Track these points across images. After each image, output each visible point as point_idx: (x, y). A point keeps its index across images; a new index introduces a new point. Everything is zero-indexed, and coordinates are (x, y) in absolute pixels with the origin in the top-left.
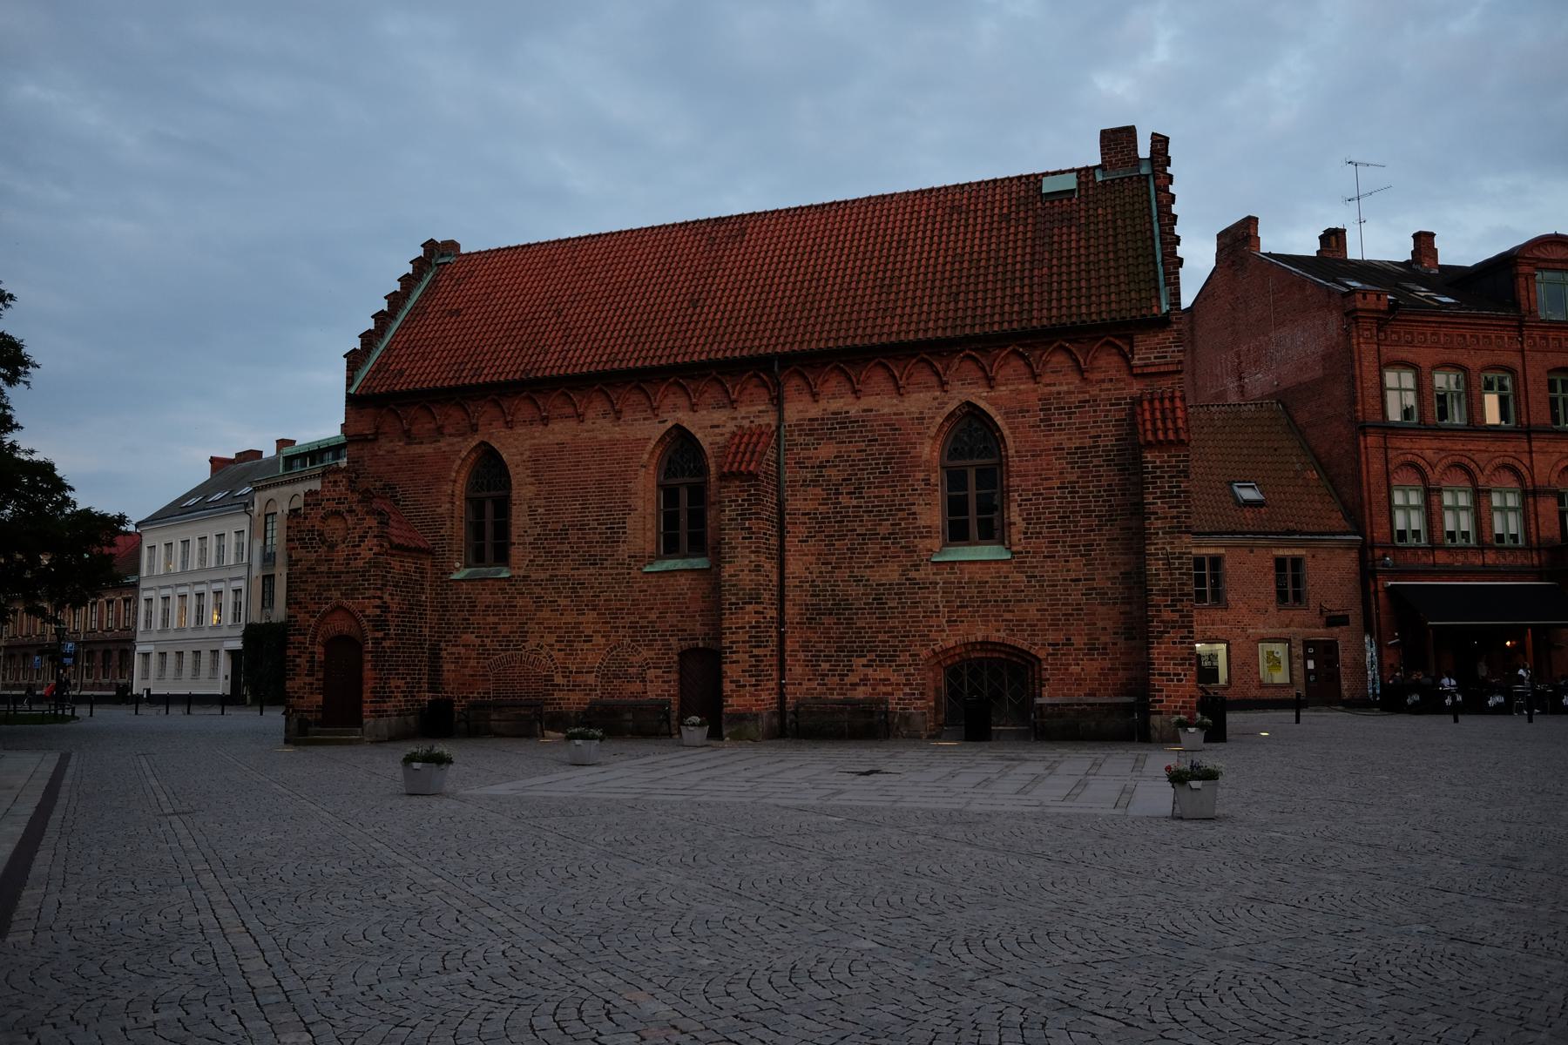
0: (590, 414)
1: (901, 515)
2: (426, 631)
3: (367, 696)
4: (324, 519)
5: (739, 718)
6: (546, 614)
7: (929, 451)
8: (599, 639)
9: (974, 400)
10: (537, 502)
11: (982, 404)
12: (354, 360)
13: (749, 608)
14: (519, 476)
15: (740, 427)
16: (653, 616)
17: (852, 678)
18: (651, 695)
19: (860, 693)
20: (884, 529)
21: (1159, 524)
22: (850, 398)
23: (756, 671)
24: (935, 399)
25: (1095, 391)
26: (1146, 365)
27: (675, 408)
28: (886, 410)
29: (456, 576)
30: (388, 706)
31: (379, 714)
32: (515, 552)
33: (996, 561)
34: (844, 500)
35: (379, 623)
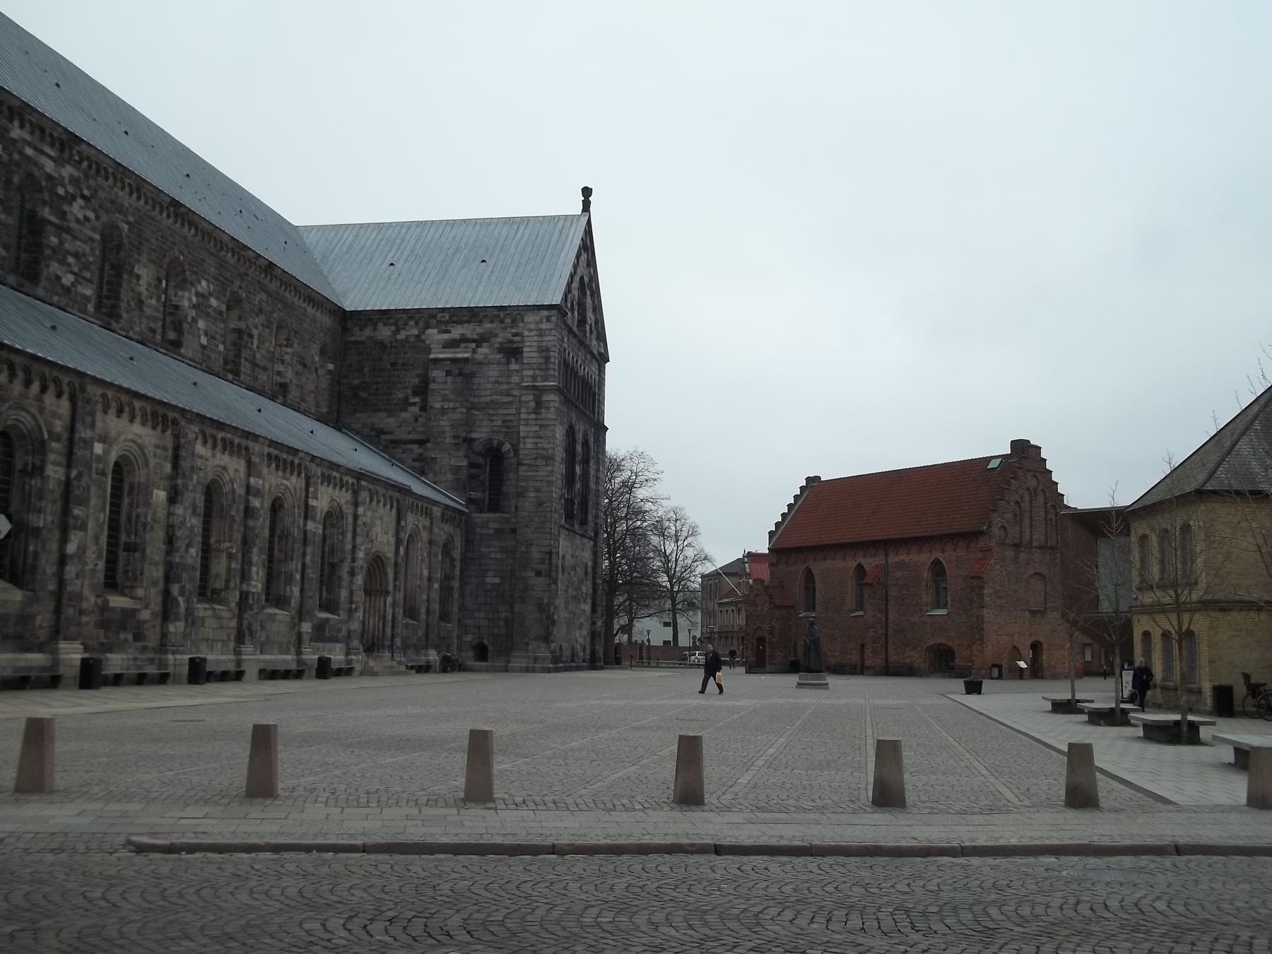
5: (868, 668)
7: (926, 575)
12: (771, 534)
14: (817, 579)
19: (908, 660)
35: (771, 633)
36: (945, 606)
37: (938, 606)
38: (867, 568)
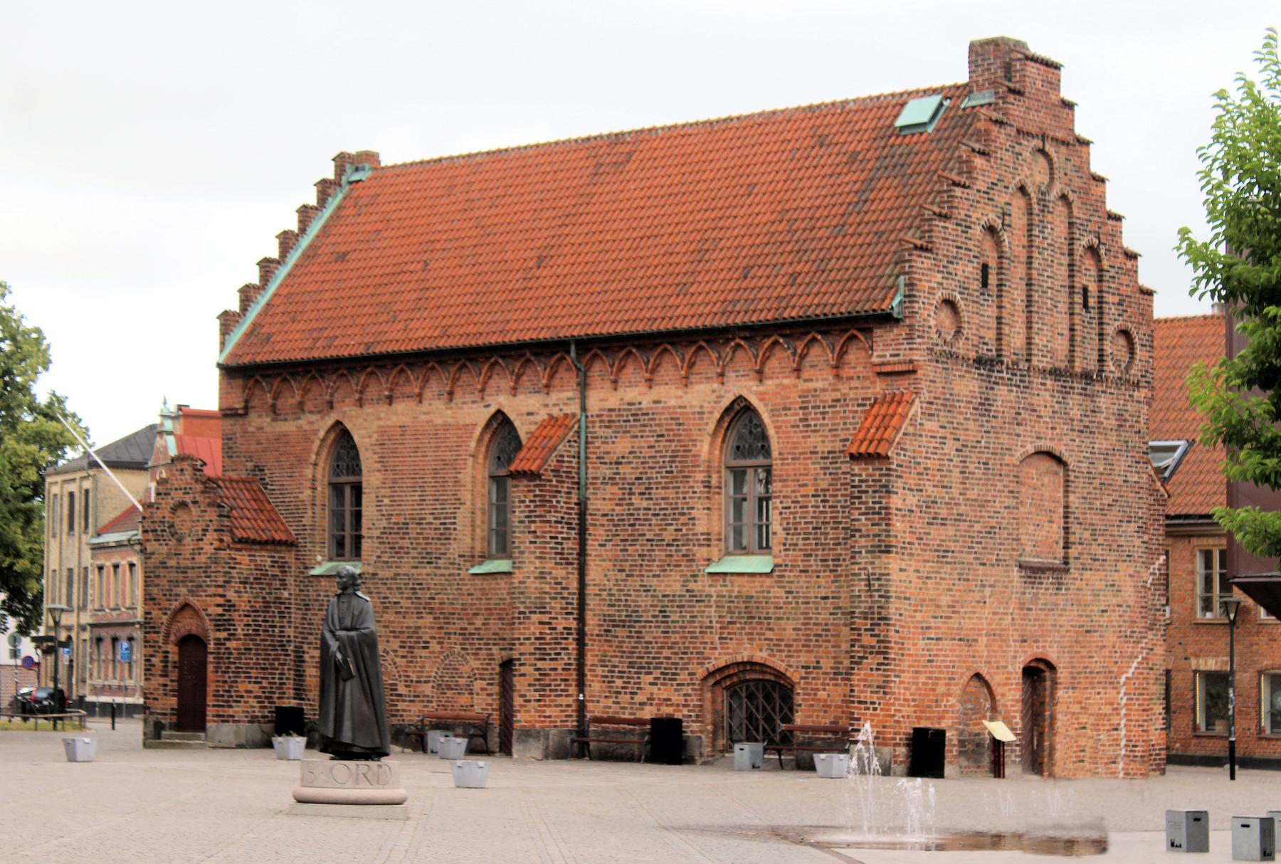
0: (428, 393)
1: (683, 519)
2: (290, 632)
3: (210, 700)
4: (174, 509)
5: (527, 734)
6: (389, 616)
7: (706, 448)
8: (434, 646)
9: (745, 394)
10: (383, 492)
11: (755, 401)
12: (228, 321)
13: (534, 618)
14: (368, 460)
15: (551, 417)
16: (479, 623)
17: (640, 698)
18: (477, 709)
20: (668, 535)
21: (863, 542)
22: (642, 388)
23: (541, 683)
24: (713, 391)
25: (844, 388)
26: (883, 364)
27: (499, 390)
28: (672, 402)
29: (317, 571)
30: (237, 710)
31: (224, 719)
32: (366, 545)
33: (761, 574)
34: (636, 500)
35: (223, 623)
36: (764, 547)
37: (741, 549)
38: (523, 428)
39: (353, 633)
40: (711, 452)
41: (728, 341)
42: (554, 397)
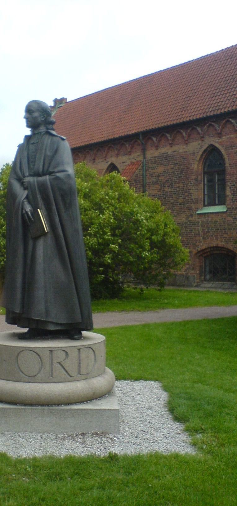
1: (186, 194)
7: (197, 167)
9: (213, 143)
11: (217, 145)
15: (132, 163)
20: (181, 200)
22: (168, 147)
27: (112, 156)
28: (181, 151)
33: (221, 212)
34: (166, 189)
36: (222, 202)
37: (212, 203)
39: (47, 178)
40: (198, 167)
41: (205, 124)
42: (132, 156)
